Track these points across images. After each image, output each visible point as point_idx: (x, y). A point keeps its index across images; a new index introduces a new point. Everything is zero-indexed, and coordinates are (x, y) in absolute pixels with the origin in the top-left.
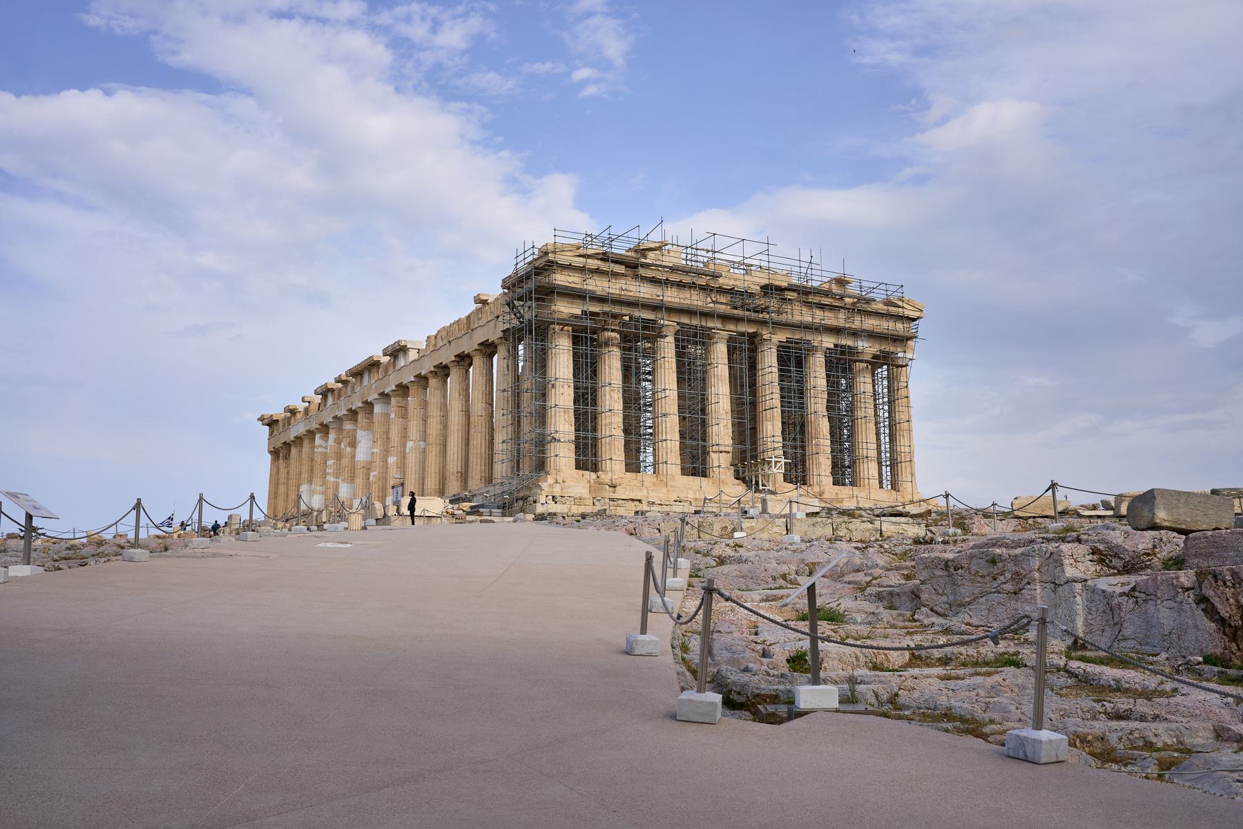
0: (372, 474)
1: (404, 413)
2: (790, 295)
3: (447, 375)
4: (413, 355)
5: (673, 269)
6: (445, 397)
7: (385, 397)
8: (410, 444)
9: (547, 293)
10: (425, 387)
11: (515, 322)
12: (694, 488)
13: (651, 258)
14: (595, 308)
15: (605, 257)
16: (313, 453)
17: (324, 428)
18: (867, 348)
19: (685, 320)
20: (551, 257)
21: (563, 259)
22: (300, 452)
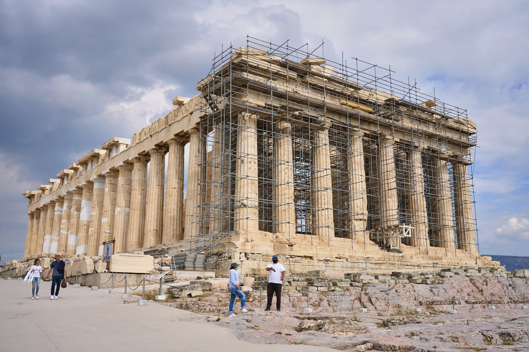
0: (90, 230)
1: (114, 188)
2: (403, 109)
3: (148, 161)
4: (122, 148)
5: (331, 80)
6: (145, 175)
7: (102, 177)
8: (118, 209)
9: (243, 85)
10: (131, 171)
11: (210, 111)
12: (341, 245)
13: (315, 69)
14: (276, 103)
15: (283, 65)
16: (54, 215)
17: (61, 200)
18: (445, 150)
19: (336, 118)
20: (244, 58)
21: (253, 61)
22: (46, 214)
